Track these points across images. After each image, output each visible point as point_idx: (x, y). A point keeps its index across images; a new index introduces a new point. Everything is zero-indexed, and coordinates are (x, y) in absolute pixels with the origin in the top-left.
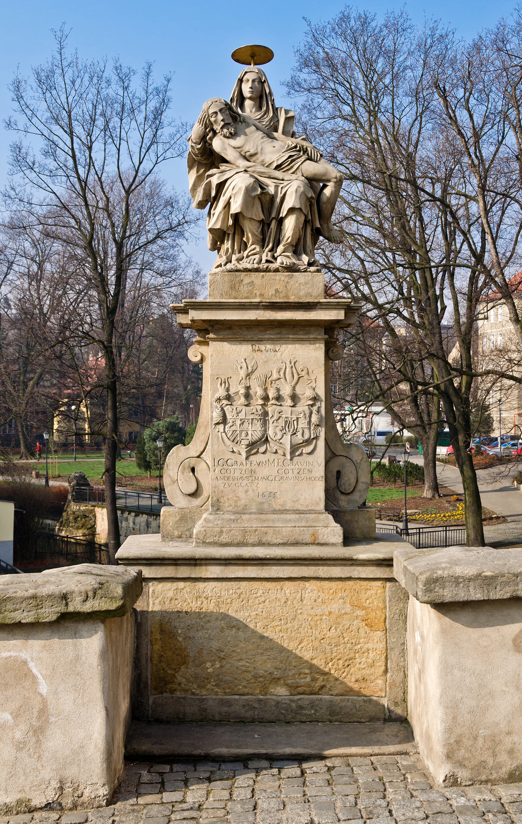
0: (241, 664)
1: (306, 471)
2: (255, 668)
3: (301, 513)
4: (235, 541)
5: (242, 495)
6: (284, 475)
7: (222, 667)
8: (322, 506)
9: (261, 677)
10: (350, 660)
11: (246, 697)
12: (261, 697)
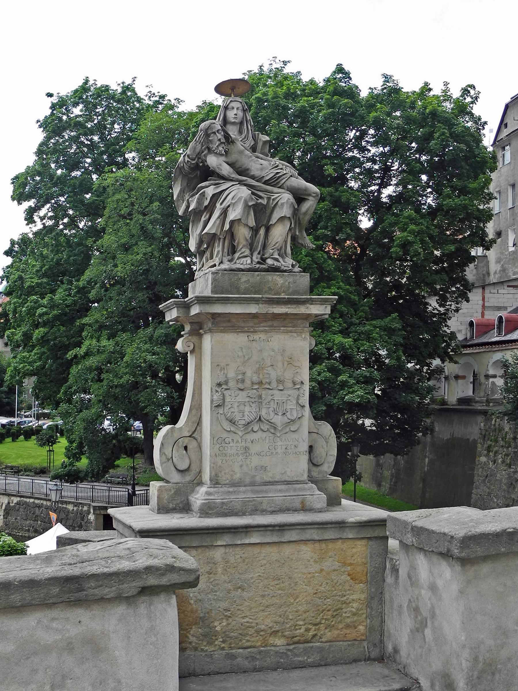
0: (245, 620)
1: (293, 447)
2: (257, 623)
3: (288, 484)
5: (237, 469)
6: (273, 451)
7: (229, 624)
8: (305, 477)
9: (262, 631)
10: (337, 610)
11: (249, 650)
12: (262, 649)
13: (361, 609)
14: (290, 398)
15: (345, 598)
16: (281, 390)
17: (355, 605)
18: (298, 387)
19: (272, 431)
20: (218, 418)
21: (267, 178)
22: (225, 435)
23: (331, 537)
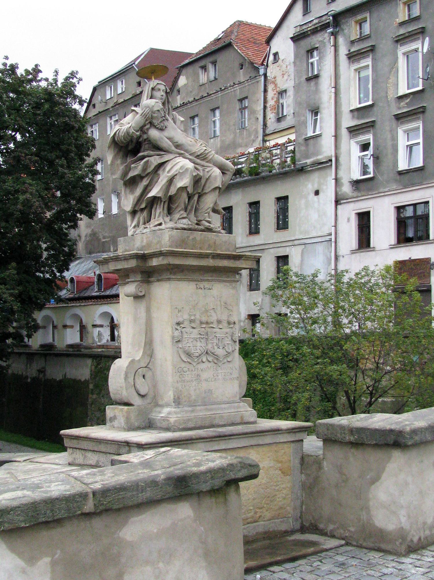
1: (229, 373)
4: (198, 426)
5: (192, 393)
6: (216, 377)
13: (288, 495)
14: (227, 335)
15: (278, 487)
16: (221, 329)
17: (284, 491)
18: (232, 326)
19: (216, 361)
20: (178, 351)
21: (199, 154)
22: (183, 365)
23: (269, 442)
